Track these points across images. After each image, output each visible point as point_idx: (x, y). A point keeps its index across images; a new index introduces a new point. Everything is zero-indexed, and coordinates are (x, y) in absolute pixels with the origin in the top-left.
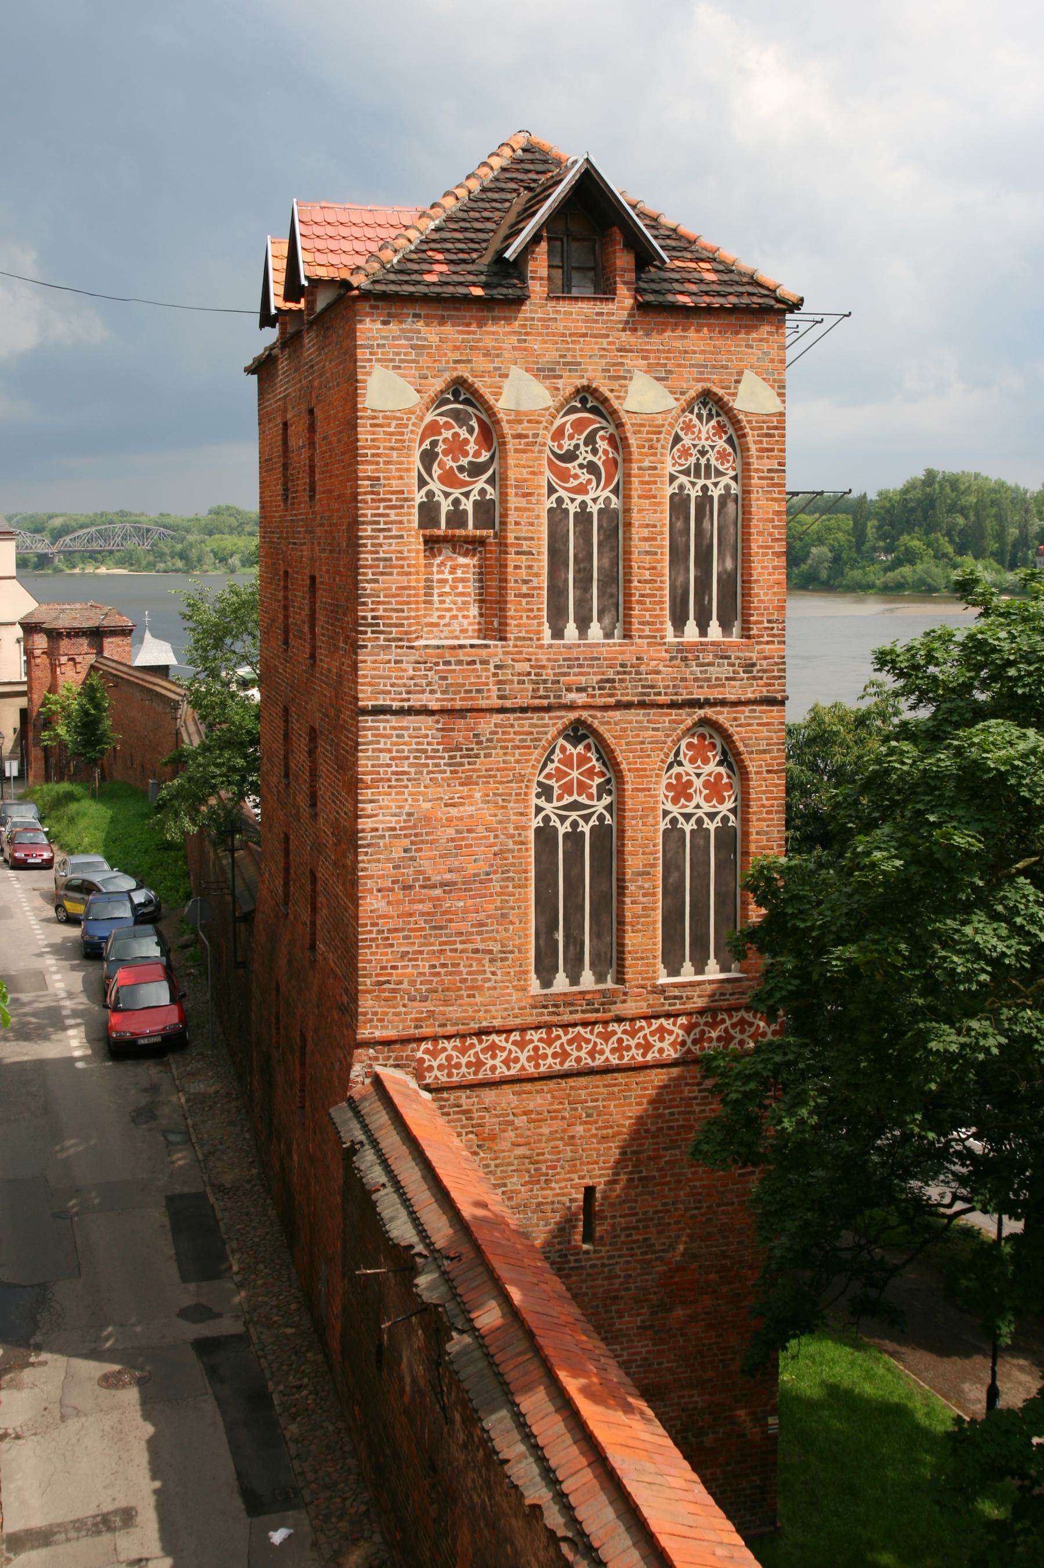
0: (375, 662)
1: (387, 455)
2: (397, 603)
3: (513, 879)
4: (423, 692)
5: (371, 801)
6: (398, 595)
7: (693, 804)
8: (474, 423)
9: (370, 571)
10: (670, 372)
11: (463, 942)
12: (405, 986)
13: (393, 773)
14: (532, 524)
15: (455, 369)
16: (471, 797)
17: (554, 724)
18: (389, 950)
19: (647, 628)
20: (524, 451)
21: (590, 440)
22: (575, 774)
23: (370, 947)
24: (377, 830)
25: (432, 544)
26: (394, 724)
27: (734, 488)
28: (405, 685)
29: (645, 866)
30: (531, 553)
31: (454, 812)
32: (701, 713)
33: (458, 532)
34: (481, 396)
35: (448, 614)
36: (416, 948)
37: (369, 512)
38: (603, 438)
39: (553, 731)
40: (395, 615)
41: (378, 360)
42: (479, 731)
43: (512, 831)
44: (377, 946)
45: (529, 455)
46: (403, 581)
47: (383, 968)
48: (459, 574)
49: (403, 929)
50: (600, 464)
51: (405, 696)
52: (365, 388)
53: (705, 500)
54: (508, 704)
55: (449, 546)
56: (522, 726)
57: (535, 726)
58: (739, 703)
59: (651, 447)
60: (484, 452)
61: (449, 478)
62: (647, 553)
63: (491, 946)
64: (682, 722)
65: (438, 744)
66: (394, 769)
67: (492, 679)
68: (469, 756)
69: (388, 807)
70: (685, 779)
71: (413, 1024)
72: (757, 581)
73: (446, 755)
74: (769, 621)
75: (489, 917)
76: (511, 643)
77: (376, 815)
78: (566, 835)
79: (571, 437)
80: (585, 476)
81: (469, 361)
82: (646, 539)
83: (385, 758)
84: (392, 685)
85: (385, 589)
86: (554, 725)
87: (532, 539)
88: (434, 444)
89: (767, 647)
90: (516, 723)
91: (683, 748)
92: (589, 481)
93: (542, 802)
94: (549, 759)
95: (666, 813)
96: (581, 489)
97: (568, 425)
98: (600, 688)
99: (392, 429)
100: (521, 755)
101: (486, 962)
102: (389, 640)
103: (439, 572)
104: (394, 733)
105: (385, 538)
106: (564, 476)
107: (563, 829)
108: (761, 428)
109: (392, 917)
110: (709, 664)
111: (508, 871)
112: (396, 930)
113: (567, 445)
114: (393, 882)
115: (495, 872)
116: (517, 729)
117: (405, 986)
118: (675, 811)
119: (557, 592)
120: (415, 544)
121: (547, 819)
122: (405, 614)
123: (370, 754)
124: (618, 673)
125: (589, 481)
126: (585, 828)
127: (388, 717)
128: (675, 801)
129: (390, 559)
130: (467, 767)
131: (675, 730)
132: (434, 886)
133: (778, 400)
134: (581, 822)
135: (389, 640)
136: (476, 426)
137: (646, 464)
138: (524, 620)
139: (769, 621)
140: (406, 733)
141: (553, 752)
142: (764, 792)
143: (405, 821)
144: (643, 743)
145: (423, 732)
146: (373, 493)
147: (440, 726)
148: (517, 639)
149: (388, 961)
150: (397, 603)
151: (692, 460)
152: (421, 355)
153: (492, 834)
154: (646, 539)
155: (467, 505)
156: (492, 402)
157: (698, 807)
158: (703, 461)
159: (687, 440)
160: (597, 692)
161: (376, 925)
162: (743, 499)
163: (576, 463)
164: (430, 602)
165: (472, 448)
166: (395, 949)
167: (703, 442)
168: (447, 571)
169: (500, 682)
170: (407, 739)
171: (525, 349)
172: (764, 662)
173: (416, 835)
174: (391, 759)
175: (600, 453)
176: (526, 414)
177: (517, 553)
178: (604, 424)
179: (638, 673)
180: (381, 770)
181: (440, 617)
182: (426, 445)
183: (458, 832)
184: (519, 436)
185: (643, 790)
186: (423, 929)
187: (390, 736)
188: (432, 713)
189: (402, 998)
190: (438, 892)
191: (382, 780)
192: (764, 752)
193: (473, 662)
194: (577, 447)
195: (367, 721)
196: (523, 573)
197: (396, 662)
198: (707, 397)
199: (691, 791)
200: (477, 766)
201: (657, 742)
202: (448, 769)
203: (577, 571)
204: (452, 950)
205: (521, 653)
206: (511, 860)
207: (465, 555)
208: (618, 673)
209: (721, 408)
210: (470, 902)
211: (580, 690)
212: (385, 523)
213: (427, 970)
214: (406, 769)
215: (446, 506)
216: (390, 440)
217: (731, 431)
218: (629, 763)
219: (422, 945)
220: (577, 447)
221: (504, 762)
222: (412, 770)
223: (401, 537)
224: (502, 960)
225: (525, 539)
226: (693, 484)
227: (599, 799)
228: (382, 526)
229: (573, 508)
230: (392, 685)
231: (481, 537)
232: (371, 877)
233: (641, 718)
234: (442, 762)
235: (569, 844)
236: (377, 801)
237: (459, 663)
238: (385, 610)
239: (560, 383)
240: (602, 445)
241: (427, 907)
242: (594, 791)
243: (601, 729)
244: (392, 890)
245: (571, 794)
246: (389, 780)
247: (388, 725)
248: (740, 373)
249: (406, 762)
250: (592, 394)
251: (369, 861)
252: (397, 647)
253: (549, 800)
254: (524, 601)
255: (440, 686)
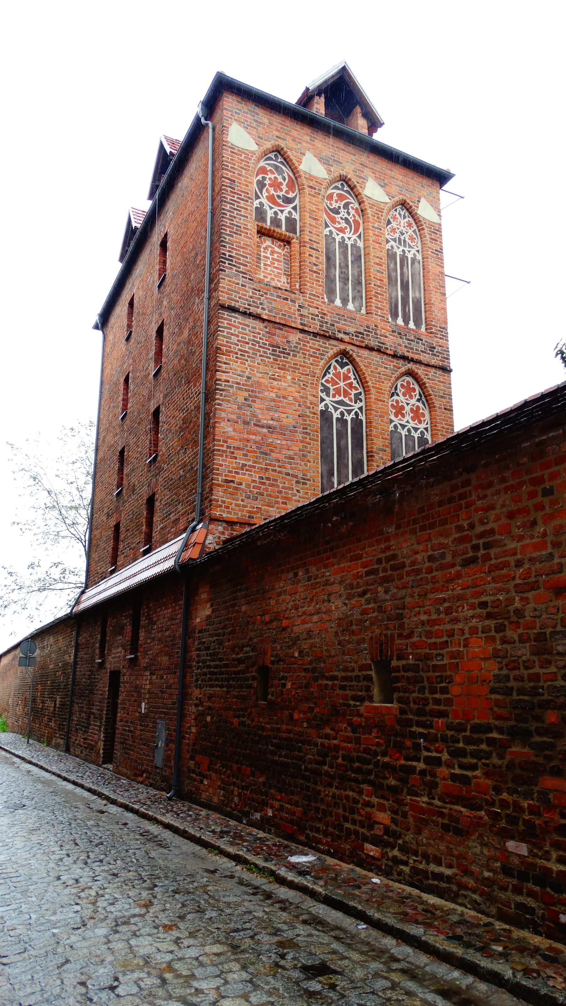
0: (230, 281)
1: (239, 171)
2: (243, 252)
3: (309, 434)
4: (258, 307)
5: (225, 363)
6: (244, 248)
7: (405, 420)
8: (286, 175)
9: (228, 229)
10: (386, 184)
11: (280, 467)
12: (243, 487)
13: (239, 350)
14: (318, 236)
15: (277, 141)
16: (285, 377)
17: (333, 348)
18: (235, 461)
19: (379, 311)
20: (314, 196)
21: (346, 206)
22: (342, 384)
23: (222, 456)
24: (228, 381)
25: (262, 232)
26: (240, 321)
27: (419, 257)
28: (247, 300)
29: (383, 446)
30: (317, 250)
31: (275, 383)
32: (410, 366)
33: (276, 230)
34: (291, 161)
35: (269, 277)
36: (251, 463)
37: (229, 197)
38: (352, 208)
39: (331, 353)
40: (242, 258)
41: (236, 120)
42: (290, 339)
43: (308, 405)
44: (226, 456)
45: (316, 199)
46: (247, 242)
47: (229, 472)
48: (275, 256)
49: (243, 449)
50: (351, 221)
51: (246, 306)
52: (228, 135)
53: (404, 258)
54: (306, 329)
55: (270, 239)
56: (315, 345)
57: (321, 346)
58: (427, 365)
59: (378, 218)
60: (291, 193)
61: (271, 198)
62: (378, 271)
63: (296, 472)
64: (399, 368)
65: (266, 340)
66: (239, 347)
67: (297, 312)
68: (284, 353)
69: (235, 370)
70: (400, 404)
71: (248, 515)
72: (433, 304)
73: (271, 348)
74: (440, 327)
75: (296, 454)
76: (308, 295)
77: (228, 372)
78: (337, 419)
79: (337, 202)
80: (344, 225)
81: (285, 140)
82: (377, 264)
83: (234, 339)
84: (240, 298)
85: (237, 242)
86: (332, 349)
87: (318, 243)
88: (264, 179)
89: (441, 340)
90: (311, 341)
91: (399, 386)
92: (346, 227)
93: (323, 395)
94: (327, 372)
95: (391, 421)
96: (342, 230)
97: (335, 195)
98: (356, 336)
99: (242, 158)
100: (313, 361)
101: (294, 483)
102: (238, 271)
103: (264, 252)
104: (241, 326)
105: (237, 214)
106: (333, 221)
107: (336, 415)
108: (431, 228)
109: (236, 440)
110: (412, 340)
111: (306, 429)
112: (239, 449)
113: (335, 205)
114: (238, 418)
115: (299, 428)
116: (311, 345)
117: (243, 487)
118: (396, 421)
119: (330, 281)
120: (252, 227)
121: (326, 406)
122: (248, 260)
123: (225, 334)
124: (366, 331)
125: (346, 228)
126: (348, 418)
127: (237, 315)
128: (396, 415)
129: (240, 227)
130: (282, 359)
131: (396, 371)
132: (263, 427)
133: (438, 217)
134: (346, 414)
135: (238, 271)
136: (287, 177)
137: (376, 225)
138: (315, 285)
139: (440, 327)
140: (247, 328)
141: (329, 368)
142: (444, 420)
143: (246, 381)
144: (379, 374)
145: (257, 331)
146: (230, 187)
147: (267, 330)
148: (310, 294)
149: (233, 468)
150: (243, 252)
151: (397, 235)
152: (259, 126)
153: (297, 404)
154: (377, 264)
155: (282, 217)
156: (297, 165)
157: (408, 422)
158: (402, 238)
159: (394, 224)
160: (355, 338)
161: (226, 442)
162: (423, 262)
163: (339, 216)
164: (259, 267)
165: (284, 187)
166: (237, 461)
167: (402, 228)
168: (269, 252)
169: (301, 315)
170: (247, 332)
171: (314, 145)
172: (440, 348)
173: (252, 391)
174: (238, 341)
175: (351, 215)
176: (315, 177)
177: (311, 248)
178: (353, 201)
179: (376, 334)
180: (232, 346)
181: (264, 276)
182: (260, 177)
183: (277, 396)
184: (311, 187)
185: (381, 401)
186: (255, 452)
187: (238, 328)
188: (264, 320)
189: (242, 496)
190: (265, 430)
191: (231, 352)
192: (442, 397)
193: (286, 299)
194: (339, 207)
195: (224, 314)
196: (314, 260)
197: (242, 285)
198: (403, 204)
199: (404, 412)
200: (288, 360)
201: (387, 375)
202: (272, 357)
203: (341, 273)
204: (273, 470)
205: (313, 303)
206: (308, 422)
207: (279, 247)
208: (366, 331)
209: (410, 213)
210: (284, 442)
211: (345, 333)
212: (238, 206)
213: (257, 479)
214: (247, 349)
215: (270, 214)
216: (241, 164)
217: (415, 227)
218: (373, 383)
219: (255, 462)
220: (339, 207)
221: (304, 362)
222: (251, 351)
223: (247, 217)
224: (304, 484)
225: (315, 242)
226: (399, 248)
227: (356, 402)
228: (235, 207)
229: (338, 239)
230: (240, 298)
231: (289, 237)
232: (225, 411)
233: (378, 359)
234: (268, 352)
235: (339, 425)
236: (228, 364)
237: (279, 297)
238: (236, 254)
239: (332, 169)
240: (352, 212)
241: (258, 438)
242: (352, 397)
243: (358, 359)
244: (237, 422)
245: (340, 396)
246: (236, 353)
247: (237, 320)
248: (420, 198)
249: (247, 345)
250: (347, 183)
251: (223, 400)
252: (243, 277)
253: (328, 395)
254: (315, 275)
255: (268, 307)
